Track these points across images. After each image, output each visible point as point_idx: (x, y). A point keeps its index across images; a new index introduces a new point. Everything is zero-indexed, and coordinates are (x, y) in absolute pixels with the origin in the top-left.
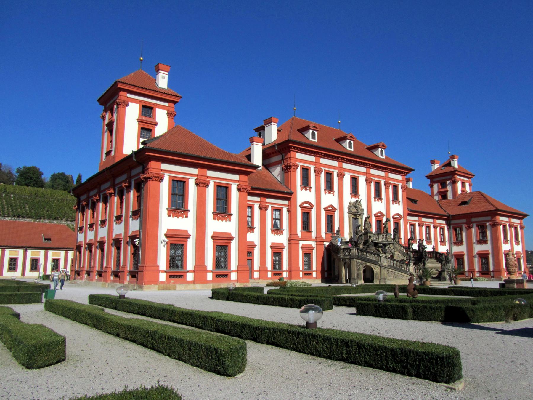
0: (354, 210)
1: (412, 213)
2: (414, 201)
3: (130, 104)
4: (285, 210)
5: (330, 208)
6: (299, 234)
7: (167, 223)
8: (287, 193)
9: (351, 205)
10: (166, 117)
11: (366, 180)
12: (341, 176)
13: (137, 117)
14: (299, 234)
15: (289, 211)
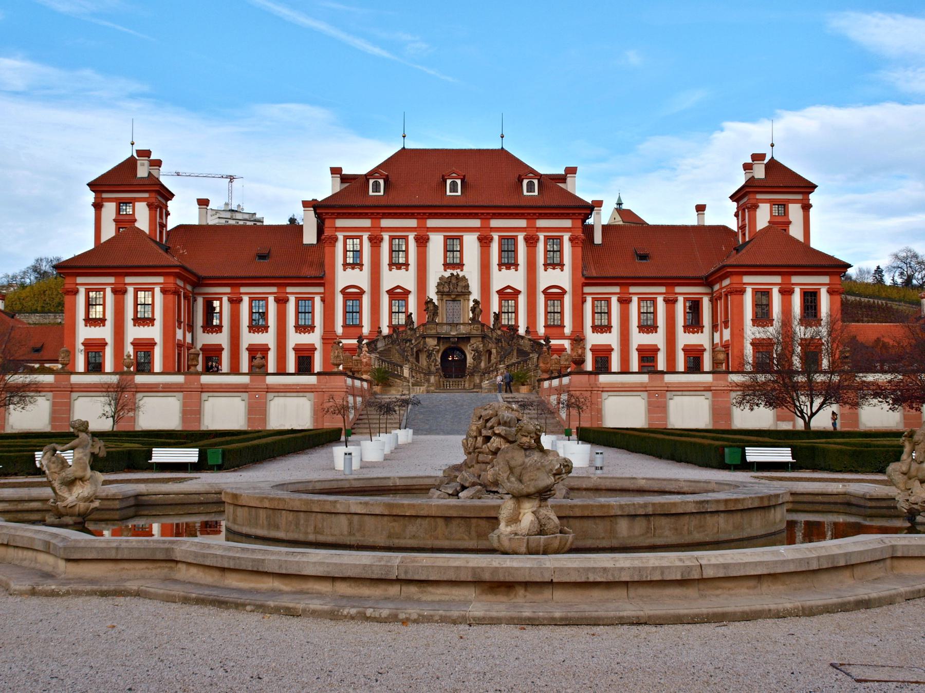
0: (446, 290)
1: (591, 281)
2: (643, 257)
3: (106, 204)
4: (317, 299)
5: (399, 290)
6: (339, 330)
7: (84, 333)
8: (316, 278)
9: (442, 282)
10: (147, 209)
11: (480, 239)
12: (422, 241)
13: (114, 216)
14: (339, 330)
15: (323, 300)
